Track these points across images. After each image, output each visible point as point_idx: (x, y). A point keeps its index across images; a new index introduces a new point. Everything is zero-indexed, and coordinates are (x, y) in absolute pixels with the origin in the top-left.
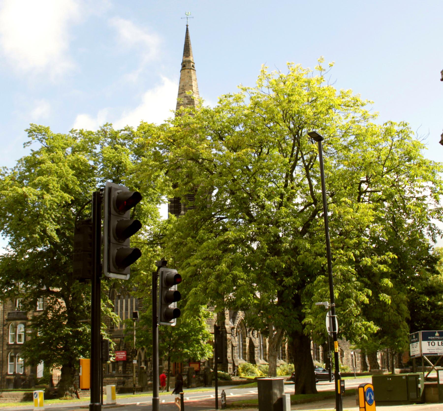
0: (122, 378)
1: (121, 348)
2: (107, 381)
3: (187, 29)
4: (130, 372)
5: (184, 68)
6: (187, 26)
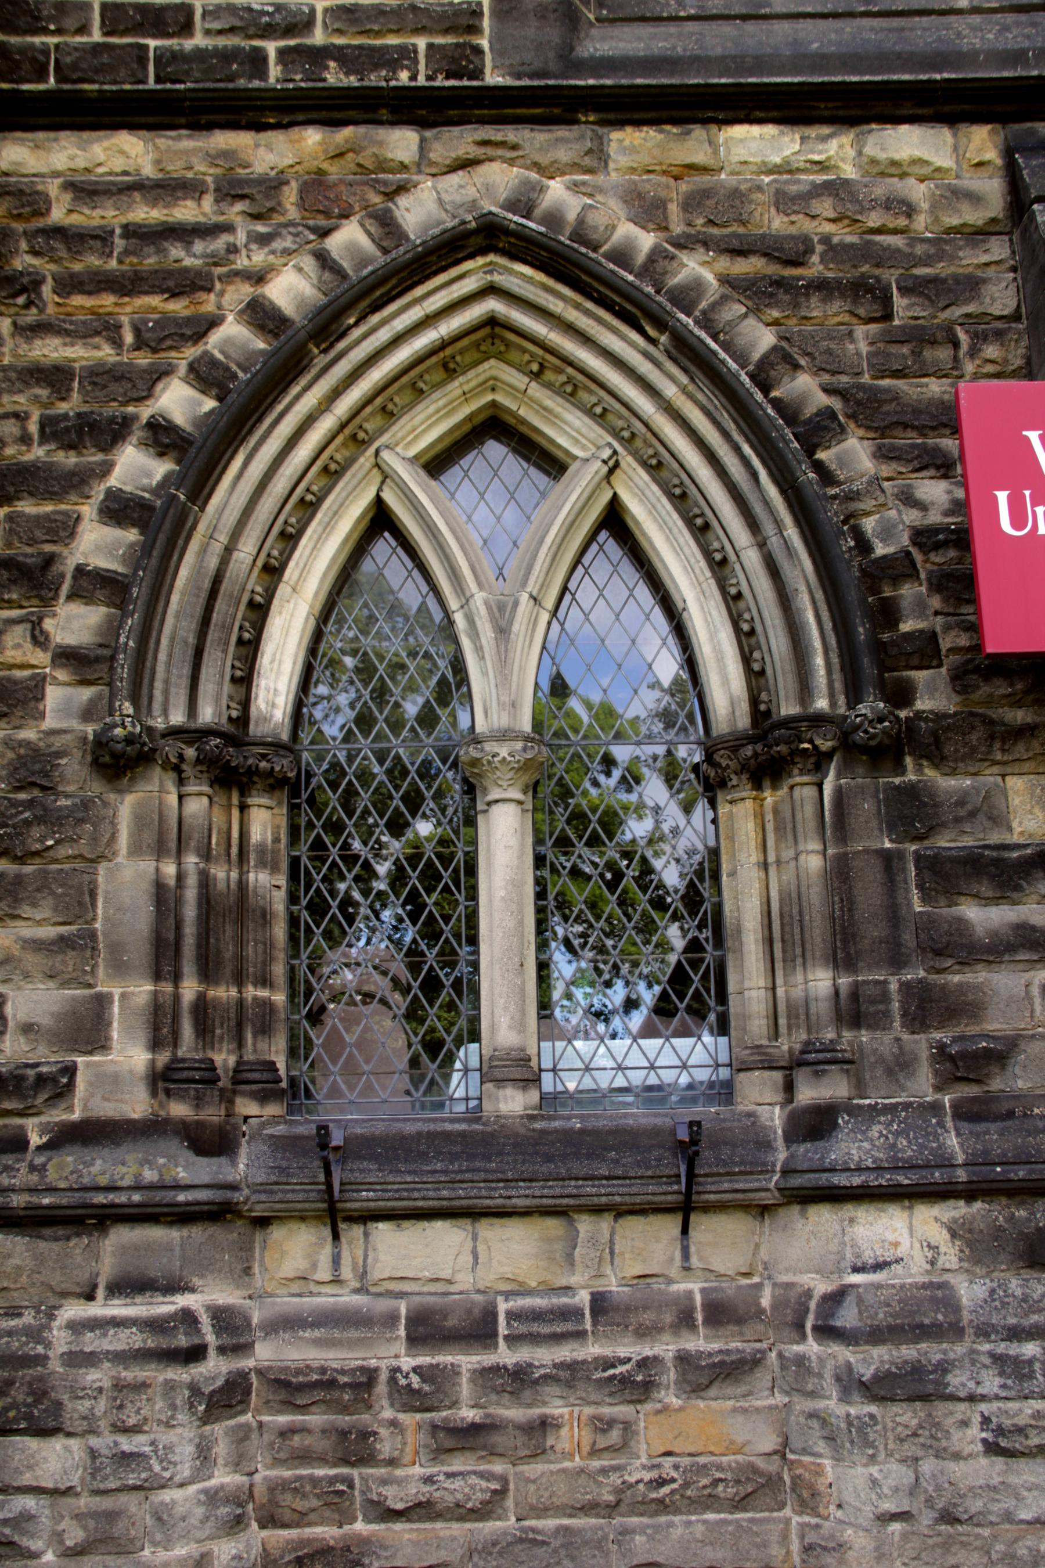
2: (427, 1328)
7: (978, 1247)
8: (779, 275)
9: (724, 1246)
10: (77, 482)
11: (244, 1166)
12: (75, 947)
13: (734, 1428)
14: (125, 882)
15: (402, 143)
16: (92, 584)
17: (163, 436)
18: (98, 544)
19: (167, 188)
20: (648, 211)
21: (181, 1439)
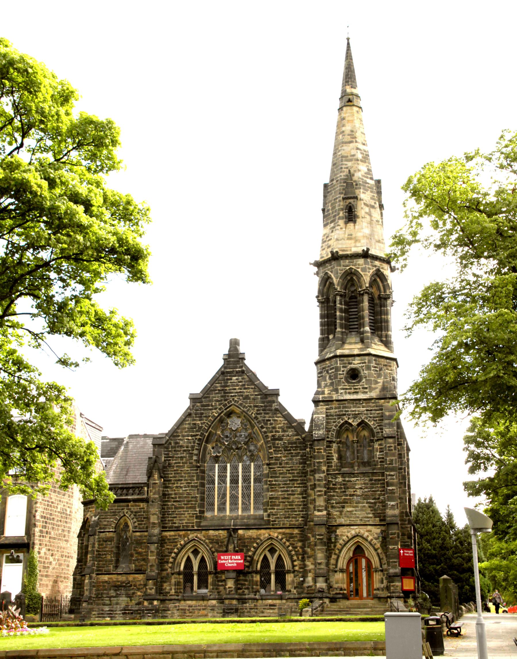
0: (234, 602)
1: (231, 547)
2: (189, 606)
3: (348, 44)
4: (246, 591)
5: (350, 104)
6: (348, 39)
7: (218, 602)
8: (212, 541)
9: (205, 602)
10: (170, 556)
11: (179, 597)
12: (170, 585)
13: (205, 612)
14: (173, 581)
15: (189, 532)
16: (171, 563)
17: (175, 553)
18: (171, 560)
19: (175, 536)
20: (204, 537)
21: (176, 612)
